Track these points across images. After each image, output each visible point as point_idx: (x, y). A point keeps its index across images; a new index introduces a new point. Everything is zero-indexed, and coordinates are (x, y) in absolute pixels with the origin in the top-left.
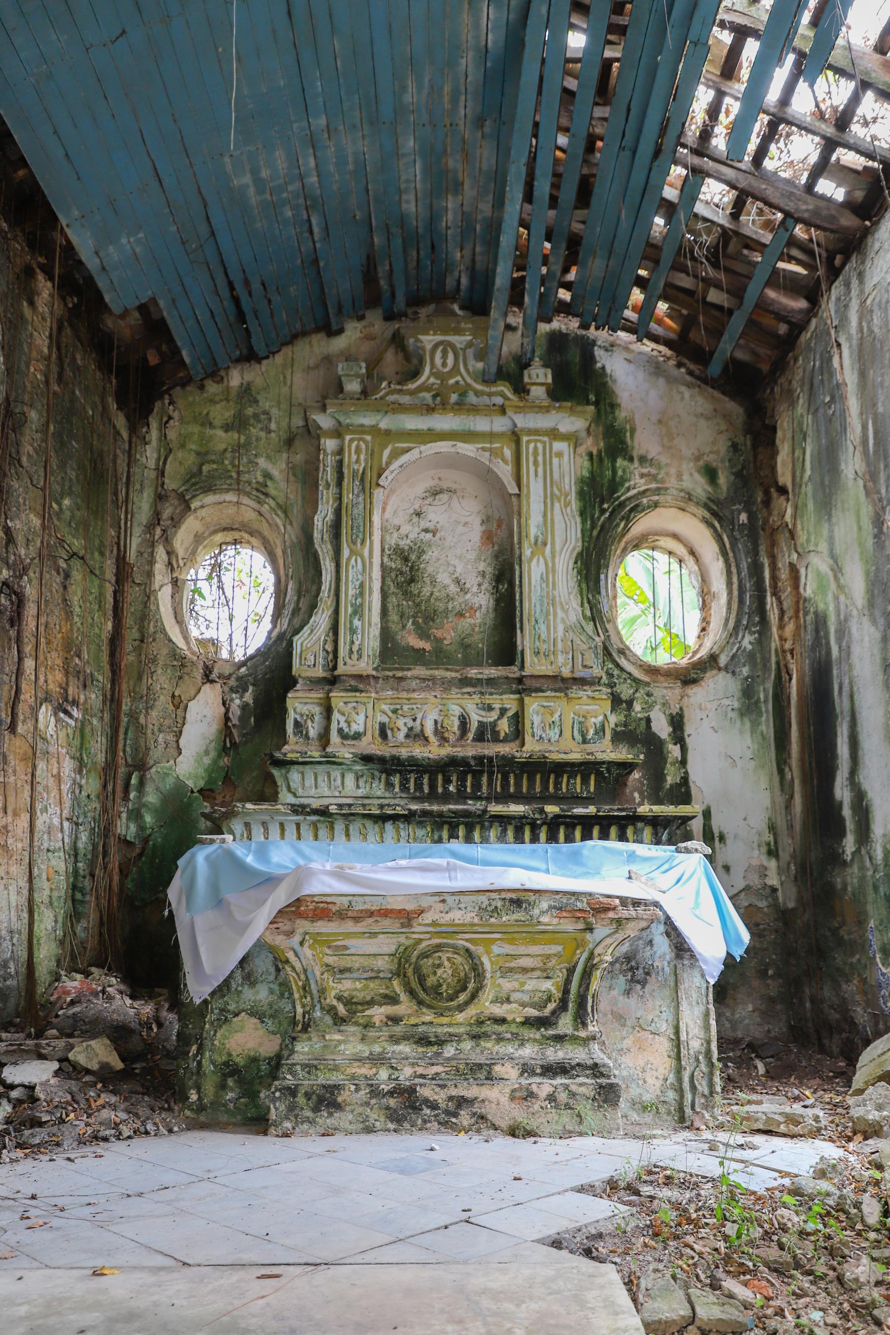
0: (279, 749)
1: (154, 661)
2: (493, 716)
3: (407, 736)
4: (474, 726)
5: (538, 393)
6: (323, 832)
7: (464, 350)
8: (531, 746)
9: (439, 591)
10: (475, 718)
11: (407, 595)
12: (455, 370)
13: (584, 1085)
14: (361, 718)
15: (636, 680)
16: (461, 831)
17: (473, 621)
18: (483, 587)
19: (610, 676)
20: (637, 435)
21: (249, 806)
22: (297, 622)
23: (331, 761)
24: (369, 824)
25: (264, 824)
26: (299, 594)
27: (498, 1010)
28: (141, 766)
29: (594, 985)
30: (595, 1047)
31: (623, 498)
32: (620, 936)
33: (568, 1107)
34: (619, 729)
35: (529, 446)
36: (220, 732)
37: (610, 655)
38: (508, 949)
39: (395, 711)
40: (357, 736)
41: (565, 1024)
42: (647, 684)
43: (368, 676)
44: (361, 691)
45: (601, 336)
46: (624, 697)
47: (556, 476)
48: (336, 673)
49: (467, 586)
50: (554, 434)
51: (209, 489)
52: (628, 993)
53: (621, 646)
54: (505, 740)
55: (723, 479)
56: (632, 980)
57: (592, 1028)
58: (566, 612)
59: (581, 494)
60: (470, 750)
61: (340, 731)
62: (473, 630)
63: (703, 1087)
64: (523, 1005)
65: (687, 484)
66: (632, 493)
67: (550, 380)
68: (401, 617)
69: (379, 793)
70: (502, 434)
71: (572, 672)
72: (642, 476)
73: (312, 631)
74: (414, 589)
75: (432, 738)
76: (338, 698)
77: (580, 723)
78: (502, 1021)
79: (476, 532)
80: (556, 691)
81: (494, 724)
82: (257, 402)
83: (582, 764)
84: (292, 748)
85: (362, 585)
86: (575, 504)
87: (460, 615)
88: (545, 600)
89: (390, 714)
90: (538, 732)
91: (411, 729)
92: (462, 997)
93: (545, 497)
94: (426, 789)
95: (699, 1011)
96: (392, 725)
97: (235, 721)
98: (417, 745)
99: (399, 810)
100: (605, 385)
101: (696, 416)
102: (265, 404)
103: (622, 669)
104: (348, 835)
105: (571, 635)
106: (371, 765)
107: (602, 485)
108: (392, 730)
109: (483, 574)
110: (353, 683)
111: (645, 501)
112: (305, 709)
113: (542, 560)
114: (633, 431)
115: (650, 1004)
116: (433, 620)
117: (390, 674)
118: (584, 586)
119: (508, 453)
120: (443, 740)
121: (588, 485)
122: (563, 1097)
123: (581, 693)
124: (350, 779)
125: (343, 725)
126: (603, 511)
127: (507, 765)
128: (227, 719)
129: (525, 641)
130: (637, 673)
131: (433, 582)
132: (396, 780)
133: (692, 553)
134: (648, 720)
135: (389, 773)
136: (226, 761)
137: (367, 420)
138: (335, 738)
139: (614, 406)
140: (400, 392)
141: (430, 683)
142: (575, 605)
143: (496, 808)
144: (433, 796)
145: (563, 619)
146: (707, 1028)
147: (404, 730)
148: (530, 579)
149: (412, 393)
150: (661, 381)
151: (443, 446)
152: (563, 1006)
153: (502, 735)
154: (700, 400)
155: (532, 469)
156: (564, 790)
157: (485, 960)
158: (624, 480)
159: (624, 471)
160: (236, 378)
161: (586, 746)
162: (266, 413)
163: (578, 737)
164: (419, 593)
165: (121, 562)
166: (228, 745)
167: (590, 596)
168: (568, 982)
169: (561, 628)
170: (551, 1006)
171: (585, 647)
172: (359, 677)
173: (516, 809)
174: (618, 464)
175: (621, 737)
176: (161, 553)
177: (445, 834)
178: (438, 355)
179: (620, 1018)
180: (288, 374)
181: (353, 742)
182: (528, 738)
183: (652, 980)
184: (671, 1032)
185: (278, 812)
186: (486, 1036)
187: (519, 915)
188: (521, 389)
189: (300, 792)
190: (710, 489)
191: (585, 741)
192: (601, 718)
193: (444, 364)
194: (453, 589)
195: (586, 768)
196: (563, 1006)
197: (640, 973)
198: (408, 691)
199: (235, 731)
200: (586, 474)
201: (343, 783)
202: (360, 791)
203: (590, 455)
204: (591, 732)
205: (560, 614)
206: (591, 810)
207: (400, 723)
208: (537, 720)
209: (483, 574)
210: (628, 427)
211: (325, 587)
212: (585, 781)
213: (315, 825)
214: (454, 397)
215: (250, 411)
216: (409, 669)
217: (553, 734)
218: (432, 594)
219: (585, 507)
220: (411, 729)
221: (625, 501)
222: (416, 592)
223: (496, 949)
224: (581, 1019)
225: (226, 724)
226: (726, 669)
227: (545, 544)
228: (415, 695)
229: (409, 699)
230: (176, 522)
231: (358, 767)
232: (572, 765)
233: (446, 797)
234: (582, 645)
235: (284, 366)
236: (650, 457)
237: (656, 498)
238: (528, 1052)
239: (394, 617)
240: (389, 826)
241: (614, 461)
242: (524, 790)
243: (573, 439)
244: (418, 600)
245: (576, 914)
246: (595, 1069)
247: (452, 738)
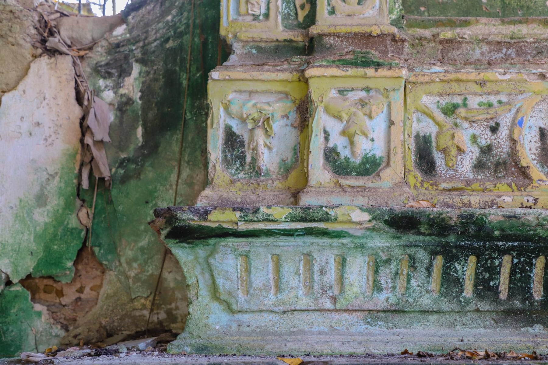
3: (479, 166)
36: (73, 156)
43: (382, 36)
44: (378, 65)
48: (314, 30)
69: (426, 301)
89: (440, 116)
91: (487, 150)
96: (445, 141)
98: (503, 187)
106: (412, 238)
108: (445, 151)
117: (427, 33)
128: (84, 129)
166: (85, 184)
181: (360, 182)
199: (100, 156)
201: (341, 279)
202: (382, 296)
216: (466, 24)
220: (487, 150)
225: (82, 141)
228: (495, 74)
229: (482, 83)
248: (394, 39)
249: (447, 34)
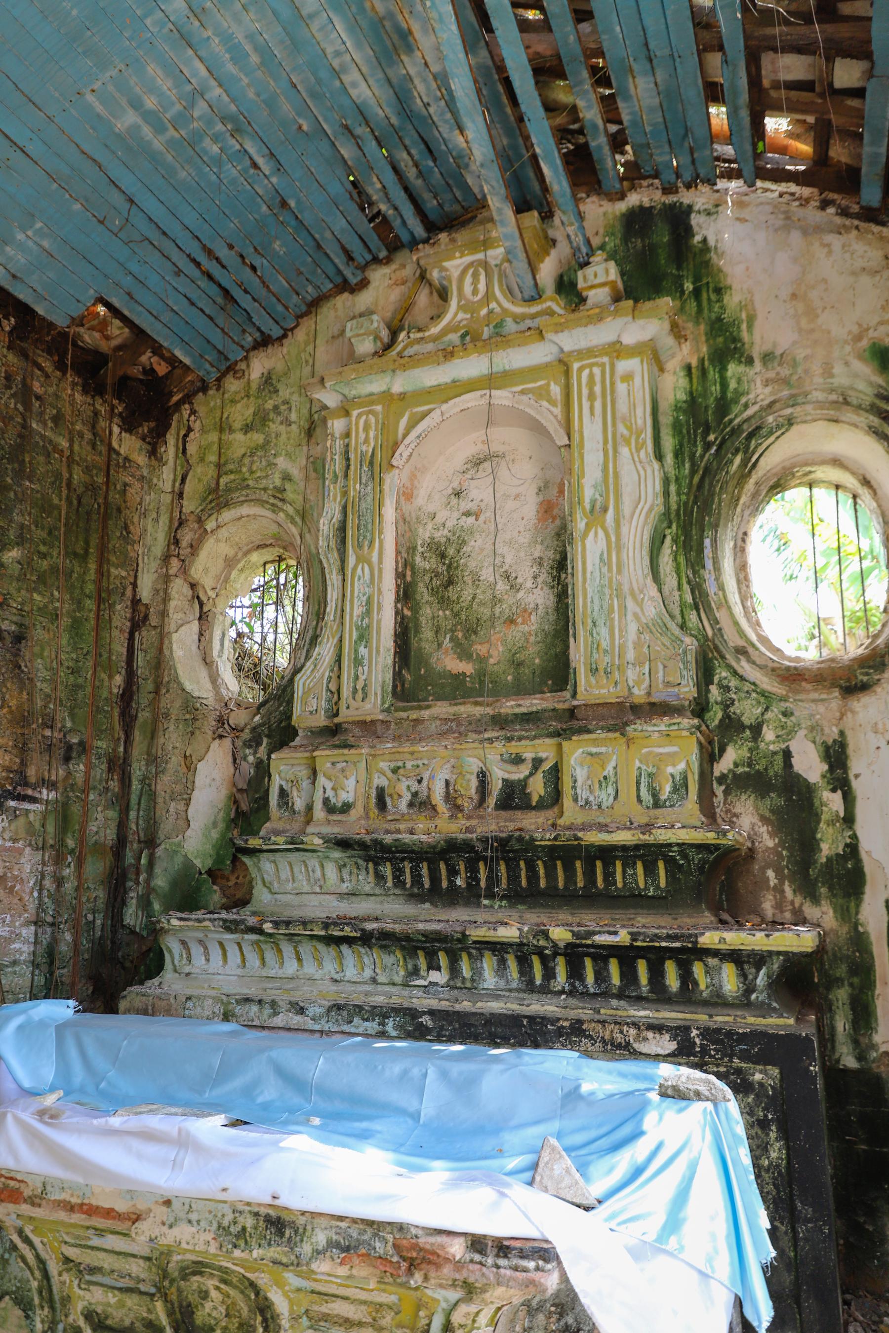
9: (484, 592)
11: (444, 602)
15: (763, 694)
17: (527, 629)
18: (540, 580)
20: (757, 324)
31: (736, 422)
34: (740, 770)
46: (746, 720)
49: (520, 580)
53: (741, 643)
54: (541, 806)
62: (527, 641)
66: (750, 412)
68: (437, 632)
71: (649, 694)
72: (766, 384)
73: (315, 666)
74: (452, 593)
77: (649, 775)
80: (609, 730)
83: (637, 847)
88: (607, 591)
90: (583, 794)
93: (606, 442)
103: (742, 678)
107: (706, 408)
109: (540, 562)
113: (601, 533)
116: (475, 633)
118: (682, 559)
121: (685, 412)
123: (650, 728)
126: (707, 446)
129: (578, 655)
130: (766, 683)
131: (476, 581)
133: (866, 482)
145: (635, 615)
148: (584, 563)
153: (535, 799)
155: (586, 405)
156: (620, 885)
158: (738, 394)
159: (739, 381)
161: (658, 812)
164: (458, 598)
167: (690, 573)
174: (729, 373)
191: (657, 804)
192: (682, 766)
194: (502, 586)
200: (683, 397)
204: (668, 788)
209: (540, 562)
210: (744, 316)
212: (650, 870)
217: (605, 796)
218: (474, 598)
219: (681, 445)
221: (739, 426)
222: (454, 598)
232: (624, 848)
236: (778, 352)
241: (723, 369)
242: (561, 884)
244: (457, 608)
248: (382, 721)
249: (414, 715)
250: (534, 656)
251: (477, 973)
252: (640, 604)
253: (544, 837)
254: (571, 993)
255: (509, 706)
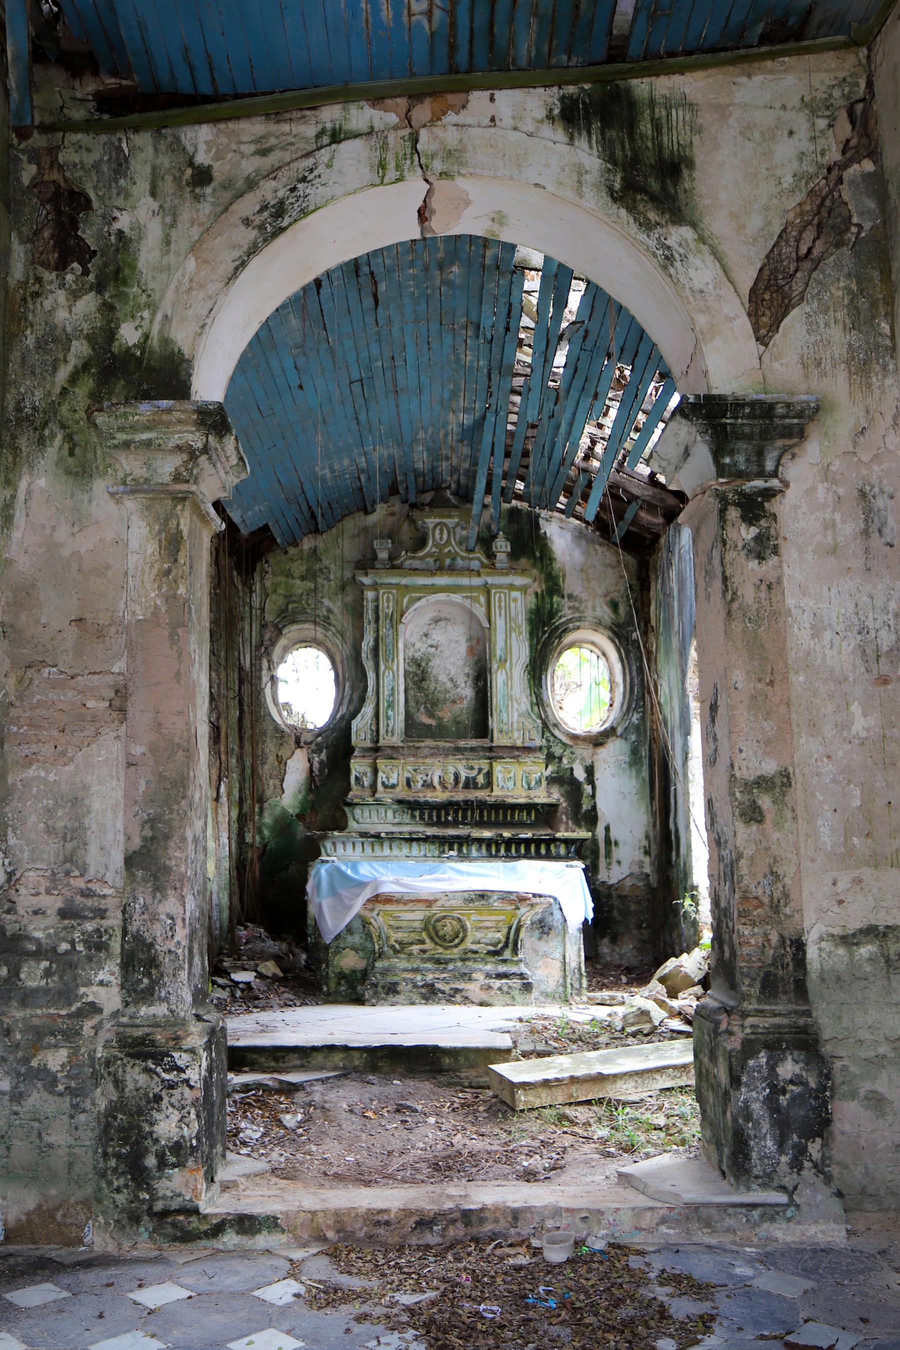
0: (347, 795)
1: (264, 733)
2: (474, 773)
4: (463, 779)
5: (502, 558)
6: (377, 848)
7: (454, 528)
8: (497, 792)
10: (463, 775)
12: (448, 542)
13: (516, 983)
14: (395, 776)
15: (564, 744)
16: (456, 847)
19: (549, 741)
21: (336, 833)
22: (352, 708)
23: (379, 803)
24: (403, 843)
25: (344, 843)
26: (353, 689)
27: (474, 947)
28: (261, 800)
29: (522, 936)
30: (522, 965)
32: (533, 912)
33: (508, 993)
35: (495, 598)
37: (548, 728)
38: (479, 918)
39: (415, 770)
40: (393, 786)
41: (507, 954)
42: (571, 746)
45: (544, 513)
46: (557, 754)
47: (513, 614)
50: (511, 587)
51: (293, 622)
52: (540, 939)
54: (482, 788)
55: (622, 610)
56: (543, 933)
57: (521, 956)
58: (519, 704)
59: (530, 621)
60: (460, 796)
61: (383, 783)
63: (577, 985)
64: (487, 944)
65: (599, 613)
67: (509, 550)
70: (479, 586)
72: (570, 608)
75: (438, 787)
76: (381, 763)
78: (476, 952)
79: (462, 648)
81: (474, 778)
82: (321, 560)
84: (355, 793)
85: (393, 689)
86: (525, 628)
87: (454, 702)
90: (501, 784)
92: (457, 941)
94: (435, 819)
95: (575, 948)
97: (316, 772)
99: (420, 836)
100: (546, 545)
101: (606, 566)
102: (326, 562)
103: (555, 737)
104: (391, 848)
105: (522, 719)
110: (389, 751)
111: (571, 626)
112: (361, 769)
114: (564, 576)
115: (551, 944)
119: (482, 599)
120: (444, 788)
122: (505, 989)
124: (390, 814)
125: (385, 780)
127: (482, 805)
129: (494, 723)
130: (565, 740)
132: (417, 813)
134: (572, 769)
135: (413, 810)
136: (311, 797)
137: (394, 580)
138: (380, 787)
139: (552, 560)
140: (413, 558)
141: (435, 752)
142: (525, 699)
143: (476, 833)
144: (439, 824)
146: (579, 956)
147: (421, 782)
149: (422, 558)
150: (583, 542)
151: (441, 596)
152: (506, 945)
154: (608, 554)
157: (468, 923)
160: (307, 544)
162: (327, 568)
163: (526, 786)
165: (241, 669)
168: (509, 933)
169: (516, 714)
170: (500, 946)
171: (530, 727)
172: (393, 748)
173: (487, 834)
175: (552, 780)
176: (265, 663)
177: (446, 848)
178: (437, 531)
179: (535, 951)
180: (340, 539)
182: (495, 787)
183: (552, 932)
184: (561, 958)
185: (352, 837)
186: (468, 959)
187: (483, 902)
188: (491, 555)
189: (361, 820)
190: (613, 616)
191: (529, 788)
193: (441, 539)
195: (529, 807)
196: (506, 945)
197: (546, 929)
198: (423, 757)
203: (536, 594)
205: (515, 705)
206: (529, 835)
207: (419, 778)
208: (500, 776)
211: (370, 689)
212: (529, 814)
213: (372, 844)
214: (448, 561)
215: (317, 566)
217: (510, 785)
223: (473, 918)
224: (515, 951)
226: (621, 736)
227: (506, 661)
228: (427, 761)
230: (273, 643)
231: (395, 807)
233: (446, 824)
234: (529, 725)
235: (338, 536)
237: (578, 624)
238: (489, 967)
239: (412, 704)
240: (414, 844)
243: (524, 589)
245: (511, 902)
246: (522, 976)
247: (450, 787)
250: (467, 719)
251: (469, 851)
252: (519, 704)
253: (491, 800)
254: (506, 857)
255: (462, 743)
